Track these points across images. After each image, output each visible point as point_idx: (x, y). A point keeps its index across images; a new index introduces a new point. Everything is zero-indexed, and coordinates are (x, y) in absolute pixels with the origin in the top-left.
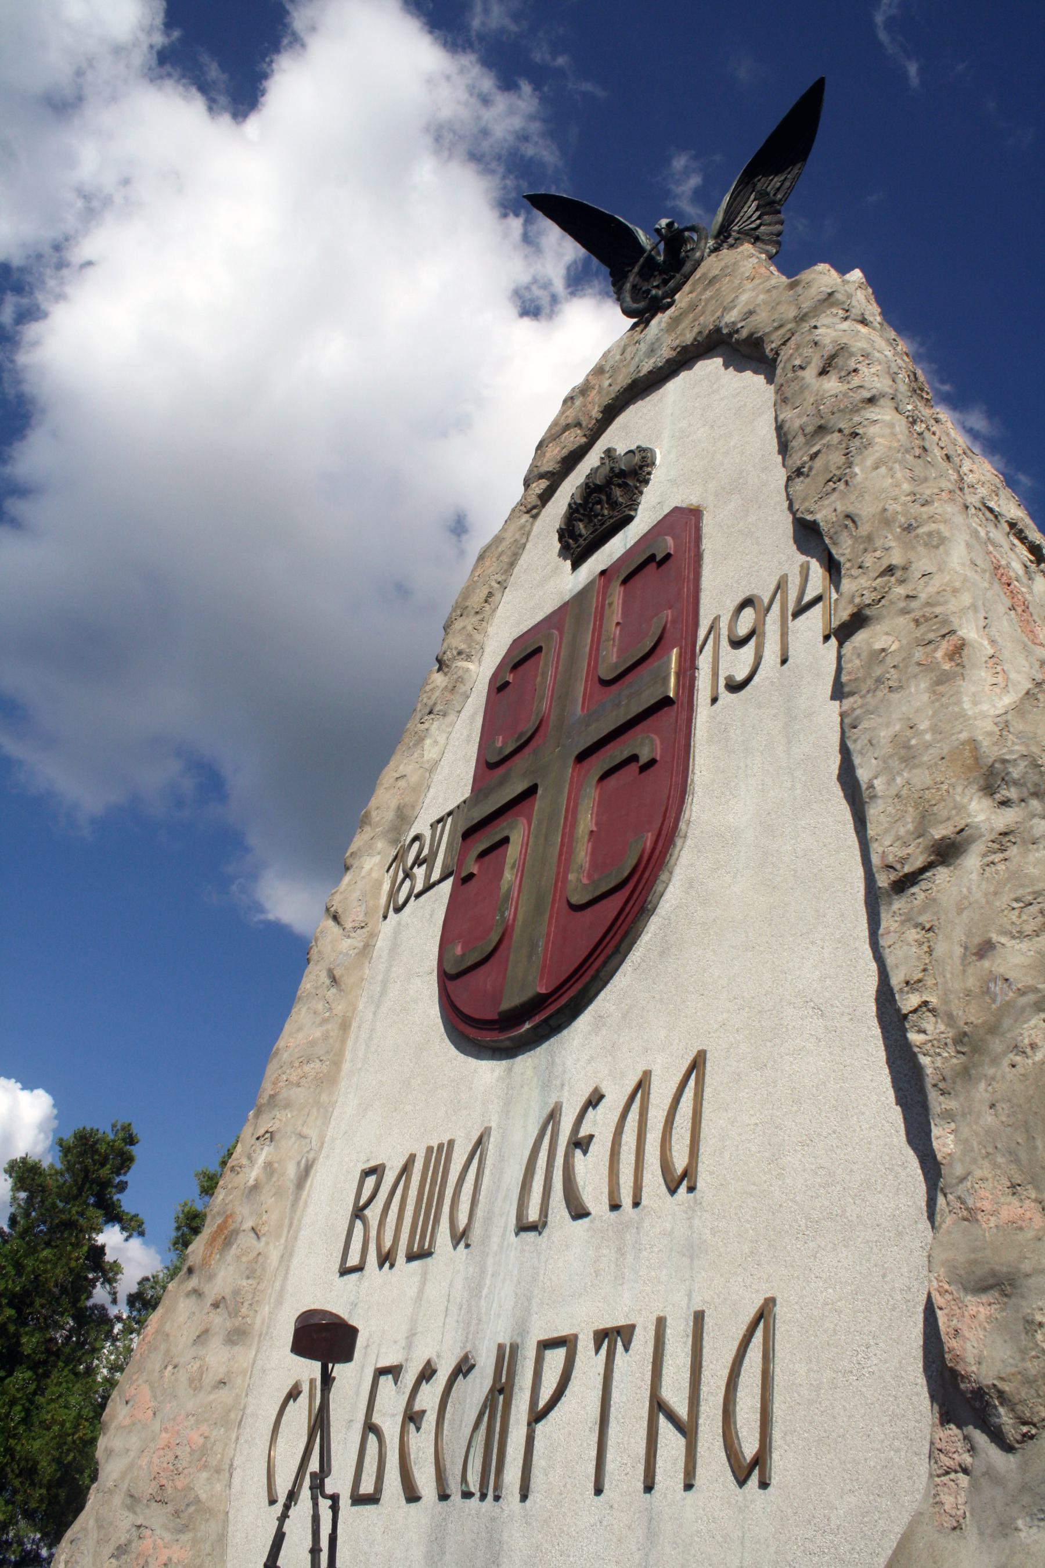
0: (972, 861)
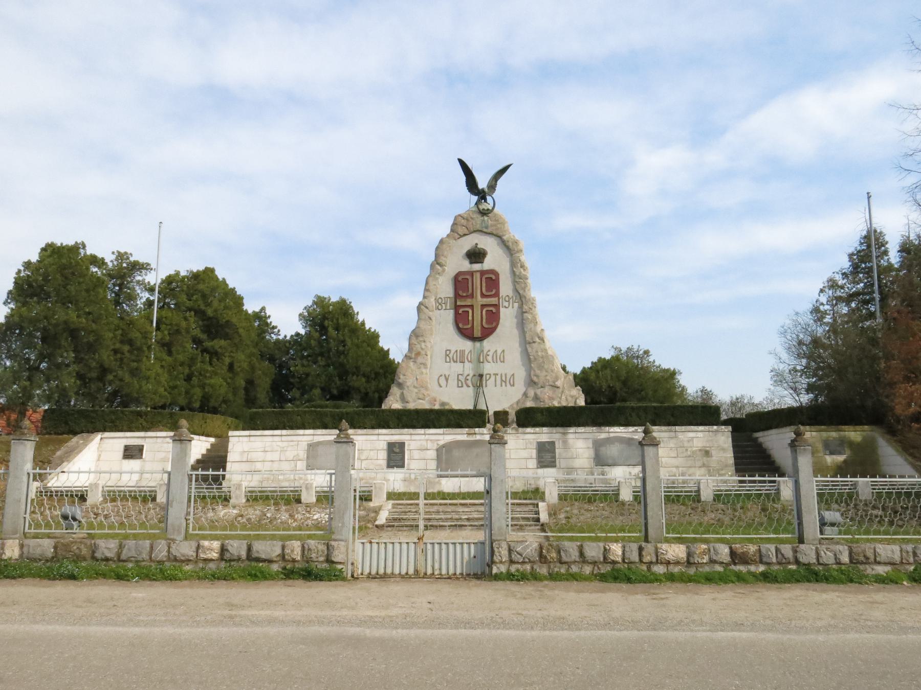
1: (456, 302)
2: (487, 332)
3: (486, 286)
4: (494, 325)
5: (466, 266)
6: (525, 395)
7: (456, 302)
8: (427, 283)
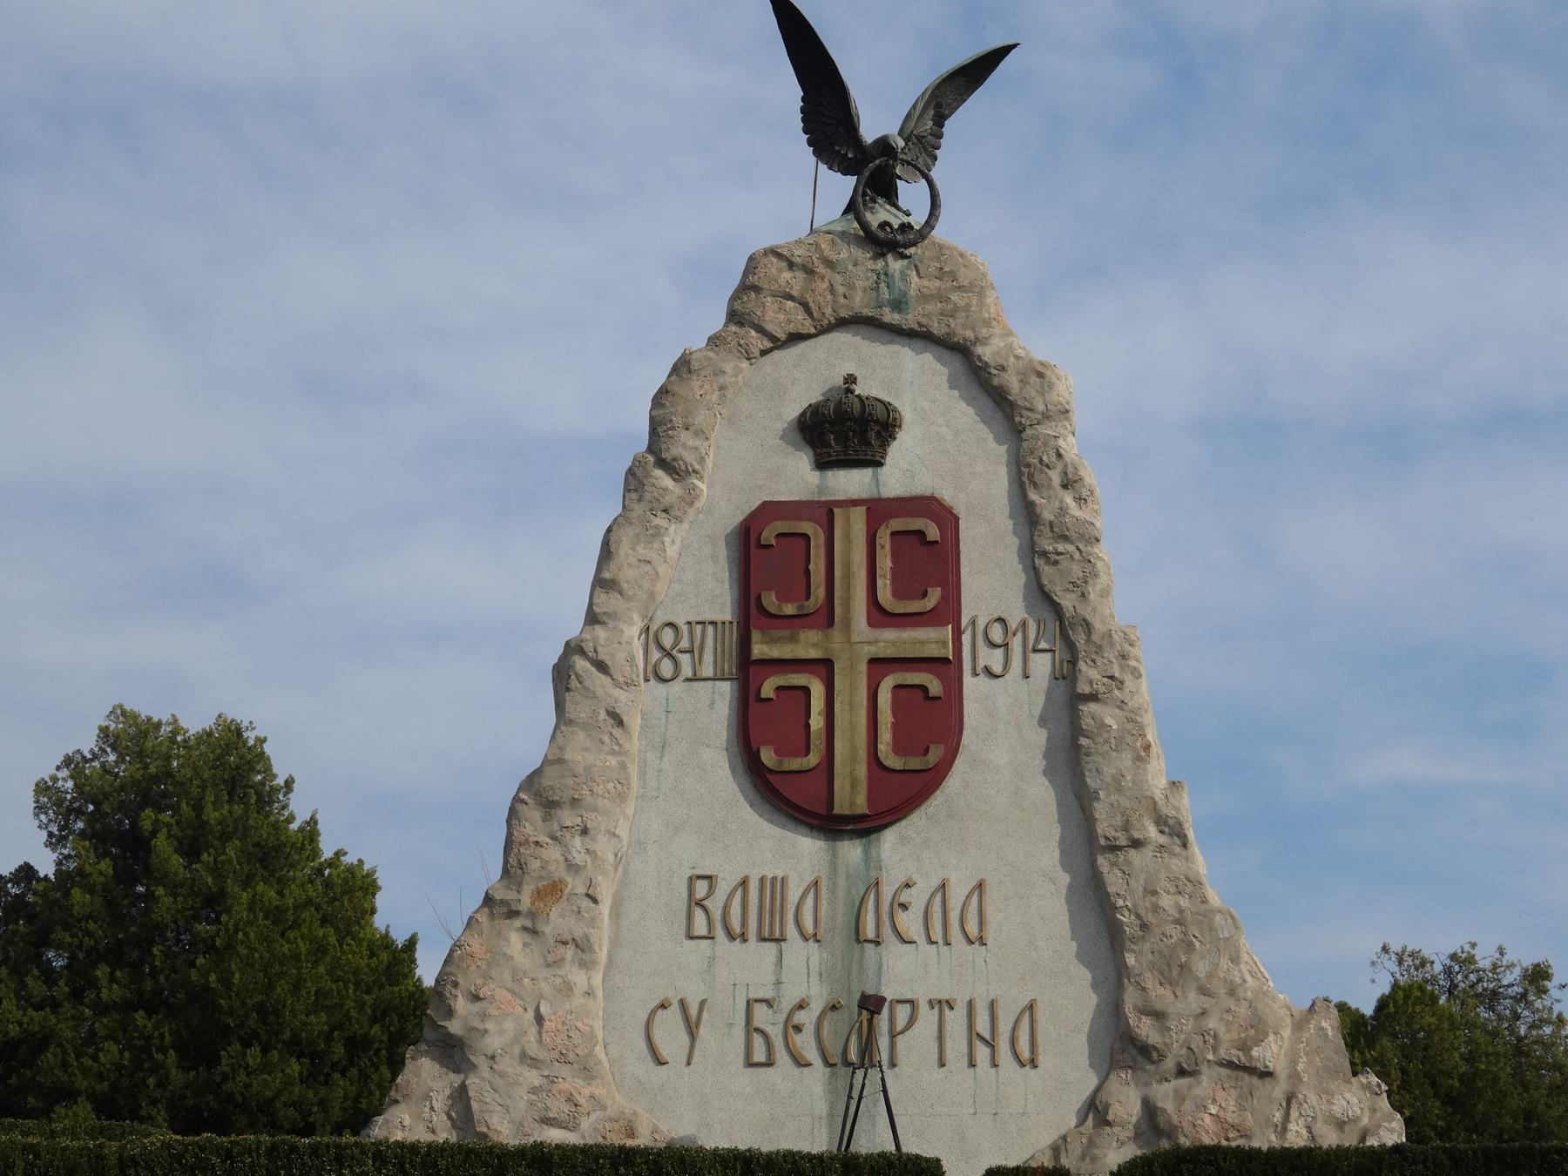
0: (1148, 852)
1: (745, 644)
2: (901, 793)
3: (896, 574)
4: (935, 755)
5: (798, 477)
6: (1096, 1110)
7: (745, 644)
8: (607, 553)
